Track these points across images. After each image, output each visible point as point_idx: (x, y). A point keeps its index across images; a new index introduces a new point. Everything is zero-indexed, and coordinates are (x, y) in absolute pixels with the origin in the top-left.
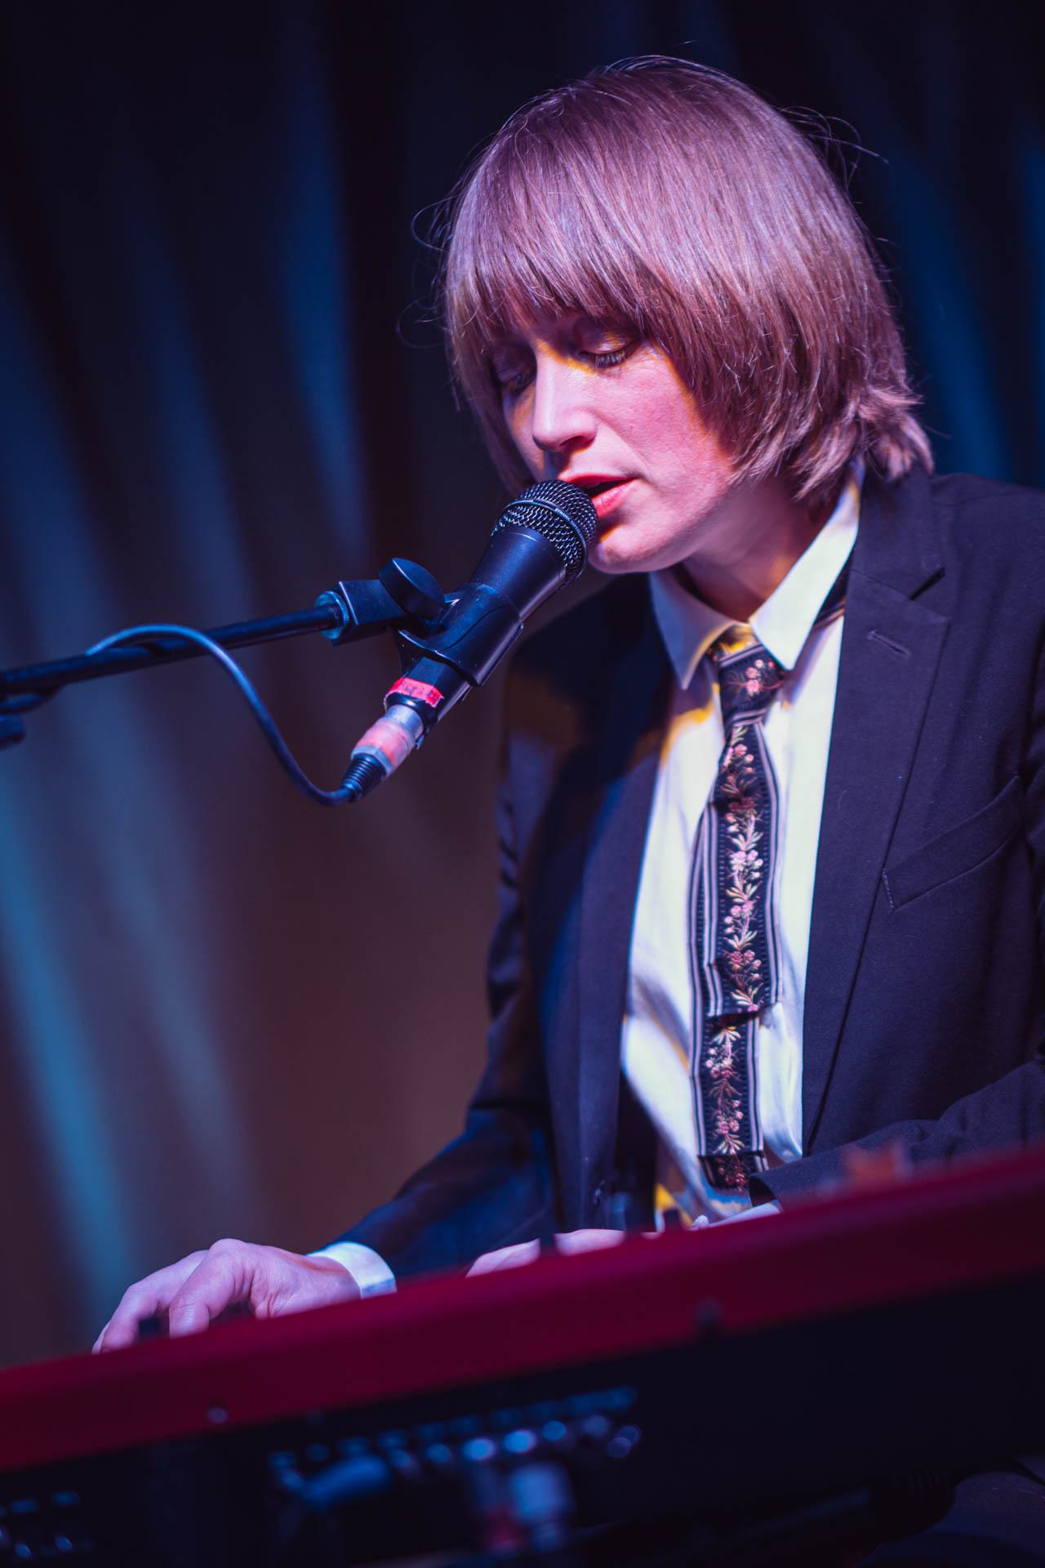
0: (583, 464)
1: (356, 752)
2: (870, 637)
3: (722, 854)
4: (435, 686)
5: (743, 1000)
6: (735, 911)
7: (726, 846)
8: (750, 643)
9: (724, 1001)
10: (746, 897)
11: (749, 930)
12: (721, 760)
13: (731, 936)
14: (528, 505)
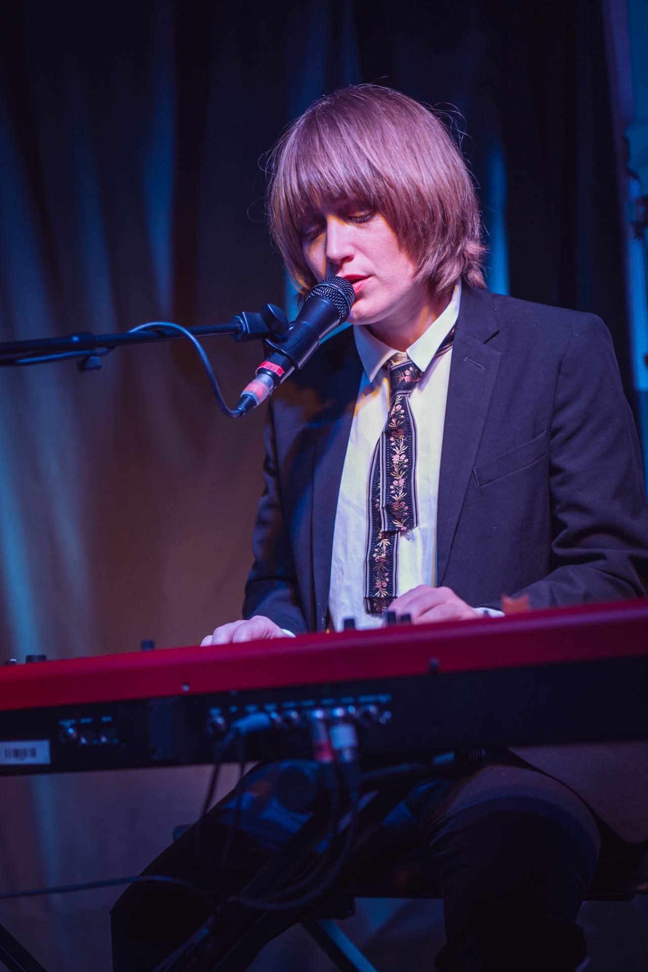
0: (349, 269)
1: (243, 393)
2: (465, 360)
3: (388, 456)
4: (281, 367)
5: (398, 524)
6: (395, 483)
7: (390, 452)
8: (405, 360)
9: (389, 525)
10: (400, 477)
11: (403, 492)
12: (390, 412)
13: (393, 495)
14: (326, 287)
